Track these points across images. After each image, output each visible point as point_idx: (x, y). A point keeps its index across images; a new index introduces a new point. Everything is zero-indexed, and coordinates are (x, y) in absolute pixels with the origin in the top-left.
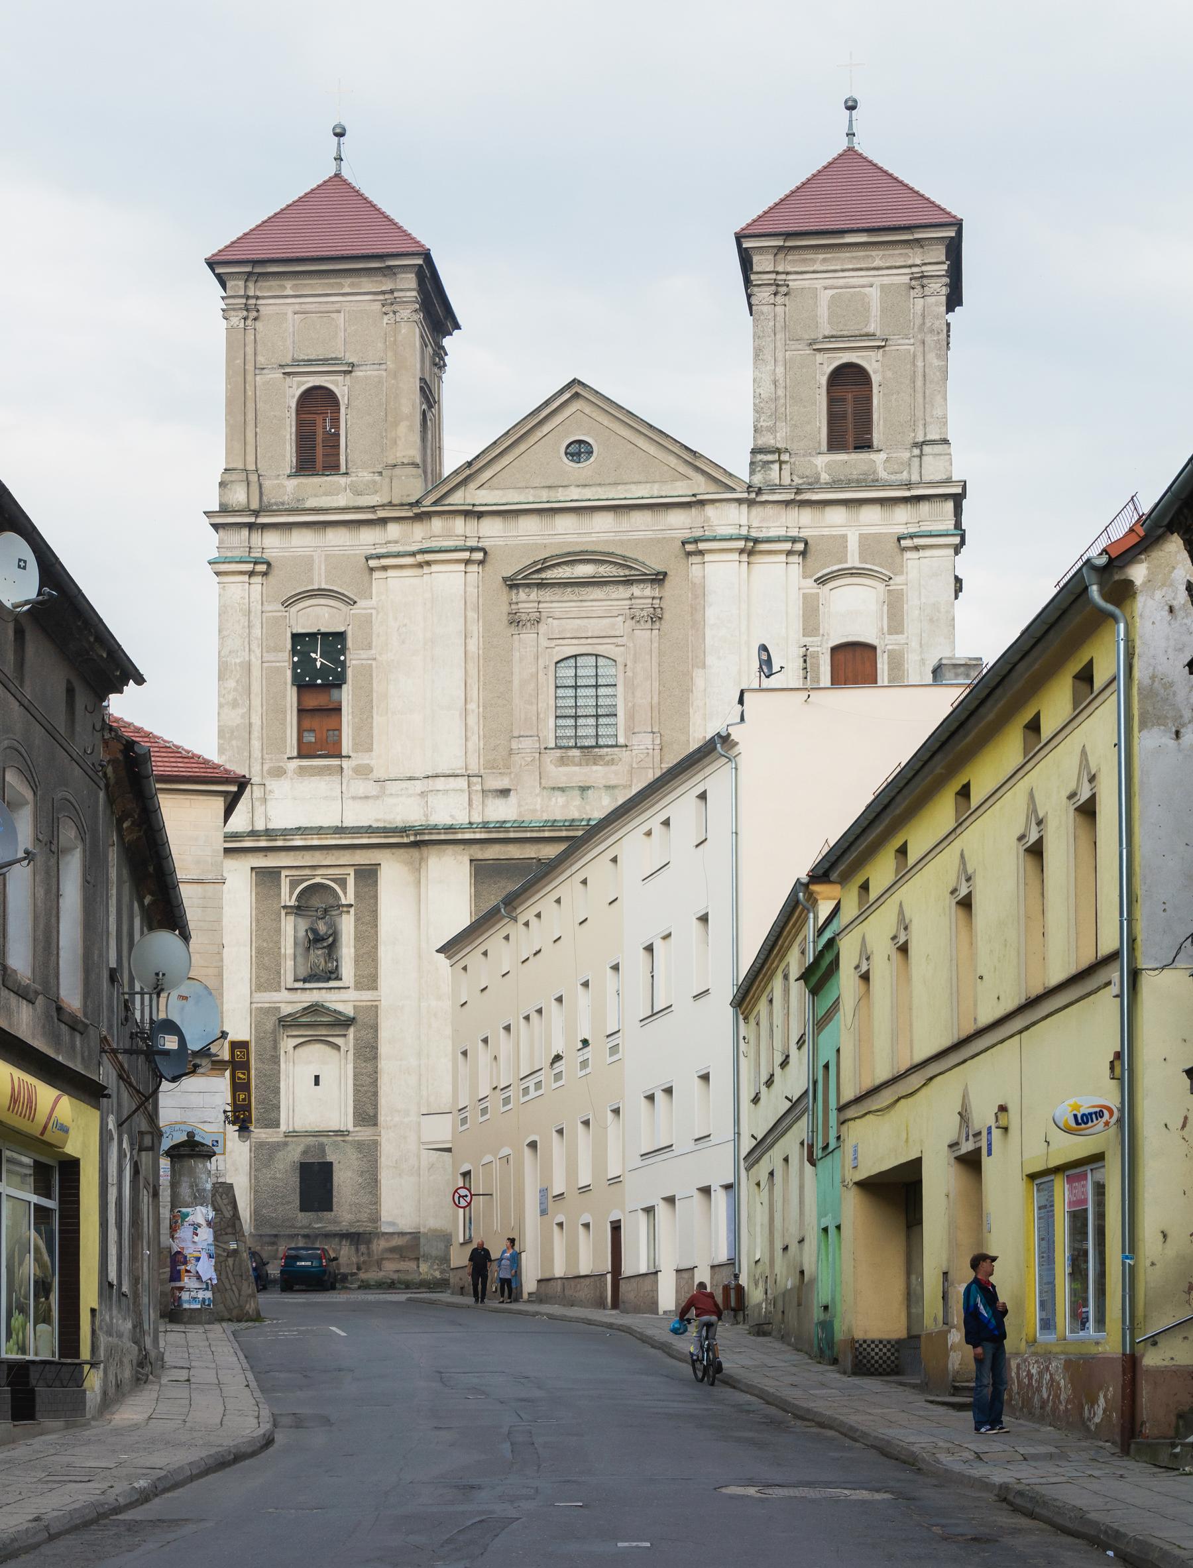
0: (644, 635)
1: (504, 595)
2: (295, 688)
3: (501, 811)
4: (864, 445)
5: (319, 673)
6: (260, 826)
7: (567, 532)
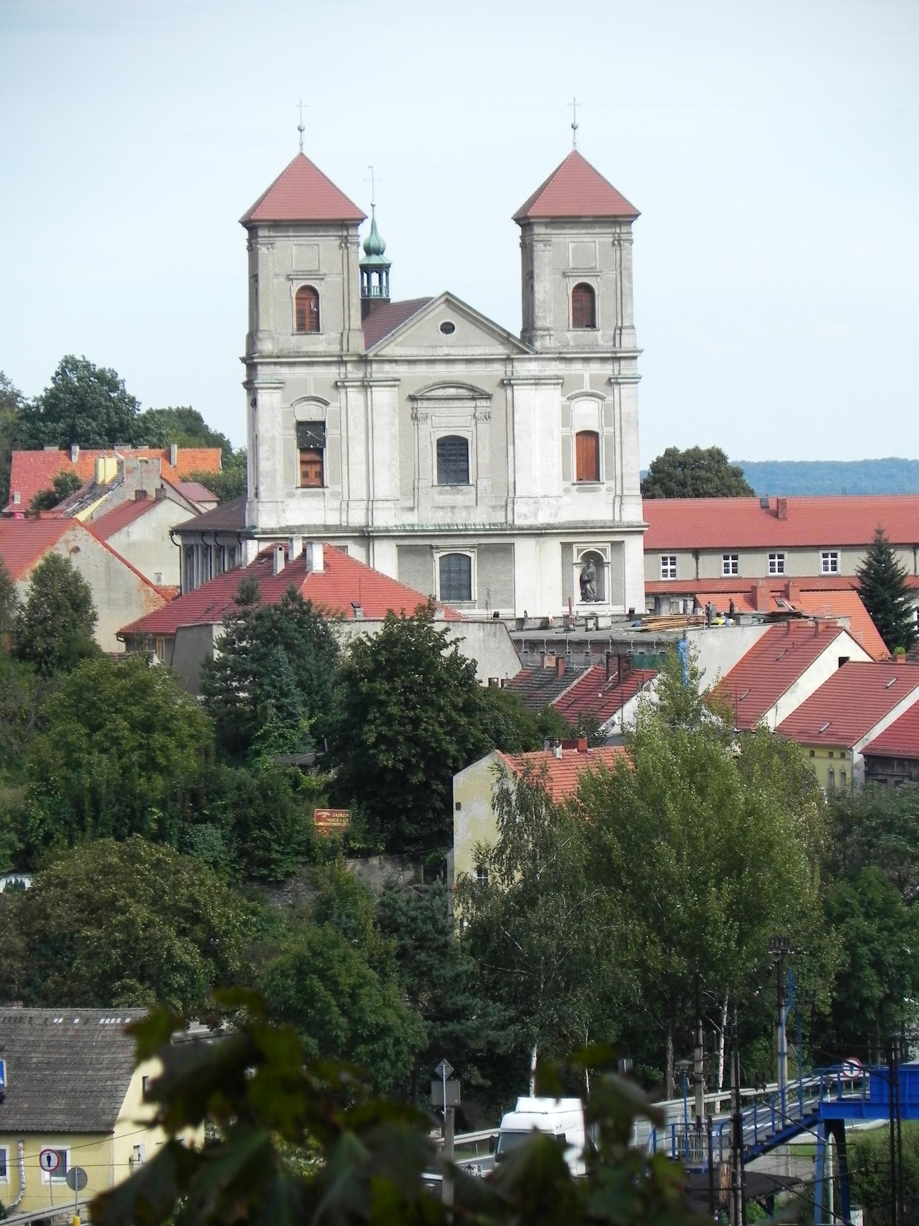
0: (483, 427)
1: (409, 405)
2: (298, 450)
3: (410, 519)
4: (592, 325)
5: (311, 440)
6: (283, 524)
7: (442, 372)
